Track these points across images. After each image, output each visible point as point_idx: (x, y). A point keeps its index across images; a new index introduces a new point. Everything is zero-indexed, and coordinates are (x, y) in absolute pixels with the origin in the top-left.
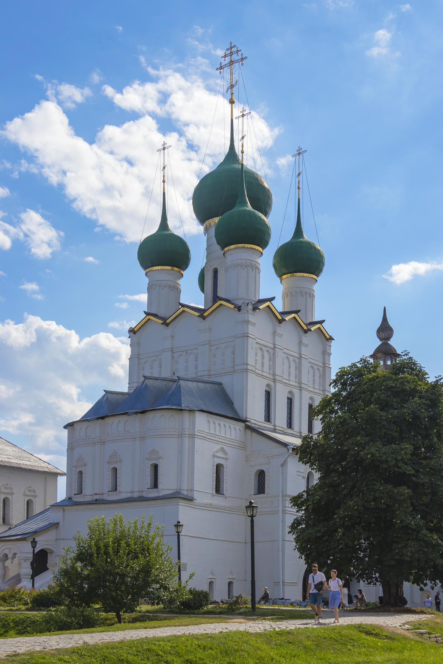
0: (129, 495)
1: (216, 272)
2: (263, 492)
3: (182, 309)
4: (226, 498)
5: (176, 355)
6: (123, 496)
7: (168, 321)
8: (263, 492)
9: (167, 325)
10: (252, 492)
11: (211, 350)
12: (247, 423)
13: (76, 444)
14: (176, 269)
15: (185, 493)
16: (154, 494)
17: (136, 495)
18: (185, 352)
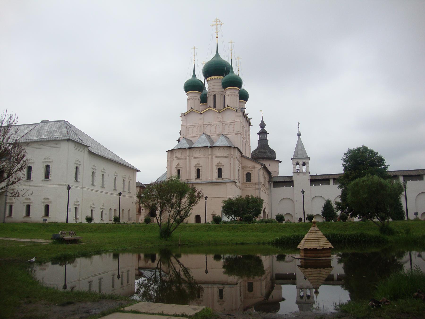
0: (205, 180)
1: (215, 96)
2: (250, 181)
3: (209, 108)
4: (239, 183)
5: (205, 126)
6: (203, 181)
7: (202, 112)
8: (251, 182)
9: (201, 114)
10: (245, 181)
11: (222, 125)
12: (242, 154)
13: (174, 159)
14: (200, 92)
15: (233, 180)
16: (220, 180)
17: (209, 181)
18: (209, 125)
